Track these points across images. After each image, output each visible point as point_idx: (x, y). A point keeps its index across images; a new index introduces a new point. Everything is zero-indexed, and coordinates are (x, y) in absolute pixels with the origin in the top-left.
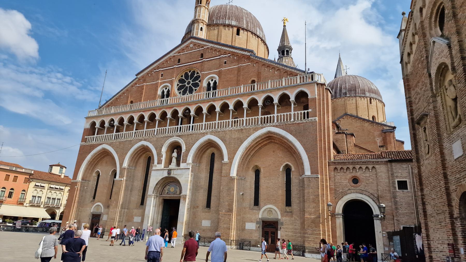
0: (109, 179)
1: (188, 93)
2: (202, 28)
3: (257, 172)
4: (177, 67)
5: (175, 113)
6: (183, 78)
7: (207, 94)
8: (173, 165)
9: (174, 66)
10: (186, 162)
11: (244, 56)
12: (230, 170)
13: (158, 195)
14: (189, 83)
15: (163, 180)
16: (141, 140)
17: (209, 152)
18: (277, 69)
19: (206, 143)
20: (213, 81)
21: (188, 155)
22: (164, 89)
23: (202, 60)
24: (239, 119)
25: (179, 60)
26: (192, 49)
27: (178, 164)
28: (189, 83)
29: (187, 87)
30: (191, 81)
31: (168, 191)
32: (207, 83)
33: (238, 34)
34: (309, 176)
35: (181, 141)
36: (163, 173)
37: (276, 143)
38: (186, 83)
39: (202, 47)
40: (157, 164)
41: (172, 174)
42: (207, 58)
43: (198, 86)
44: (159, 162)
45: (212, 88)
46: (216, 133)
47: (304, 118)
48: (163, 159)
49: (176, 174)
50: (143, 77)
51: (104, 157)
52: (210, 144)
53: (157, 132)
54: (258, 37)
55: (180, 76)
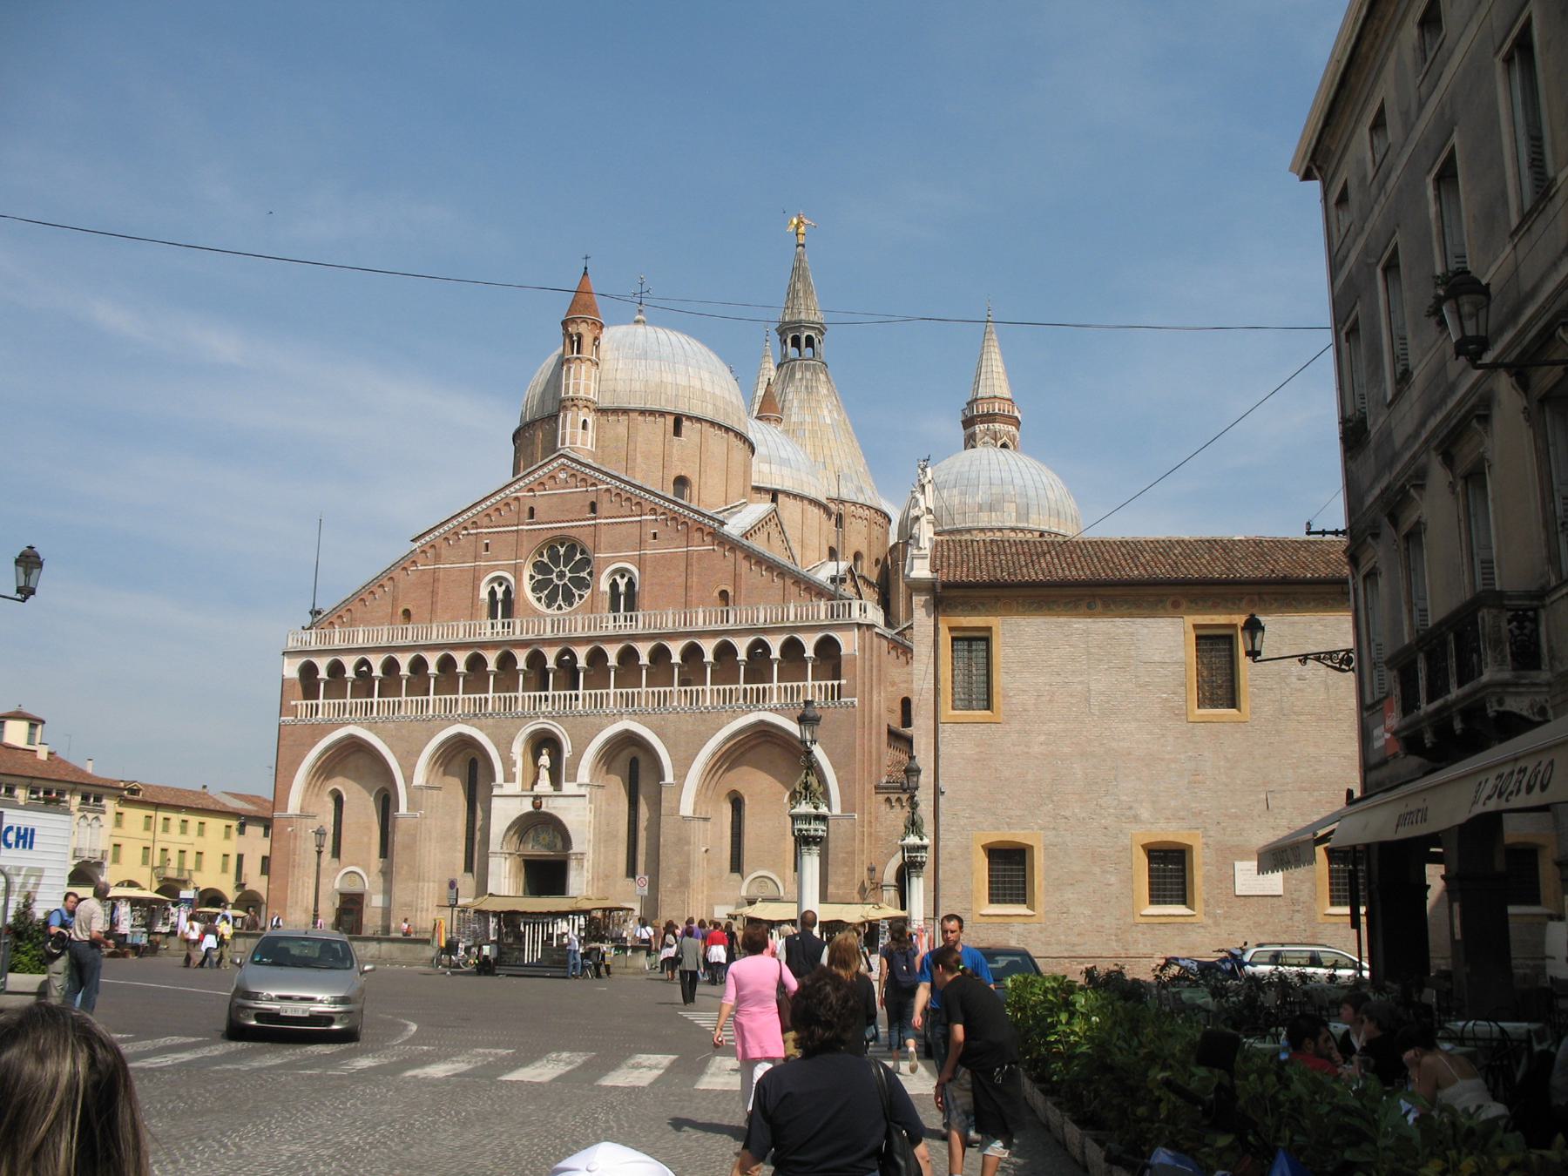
2: (585, 421)
3: (737, 803)
4: (527, 531)
5: (536, 660)
6: (545, 559)
9: (520, 527)
14: (561, 575)
16: (456, 721)
22: (496, 587)
23: (595, 519)
24: (694, 688)
25: (532, 510)
28: (562, 575)
29: (558, 586)
33: (677, 431)
37: (775, 743)
39: (594, 485)
44: (510, 777)
45: (622, 597)
47: (833, 698)
48: (518, 770)
51: (347, 756)
52: (628, 740)
53: (494, 702)
54: (727, 429)
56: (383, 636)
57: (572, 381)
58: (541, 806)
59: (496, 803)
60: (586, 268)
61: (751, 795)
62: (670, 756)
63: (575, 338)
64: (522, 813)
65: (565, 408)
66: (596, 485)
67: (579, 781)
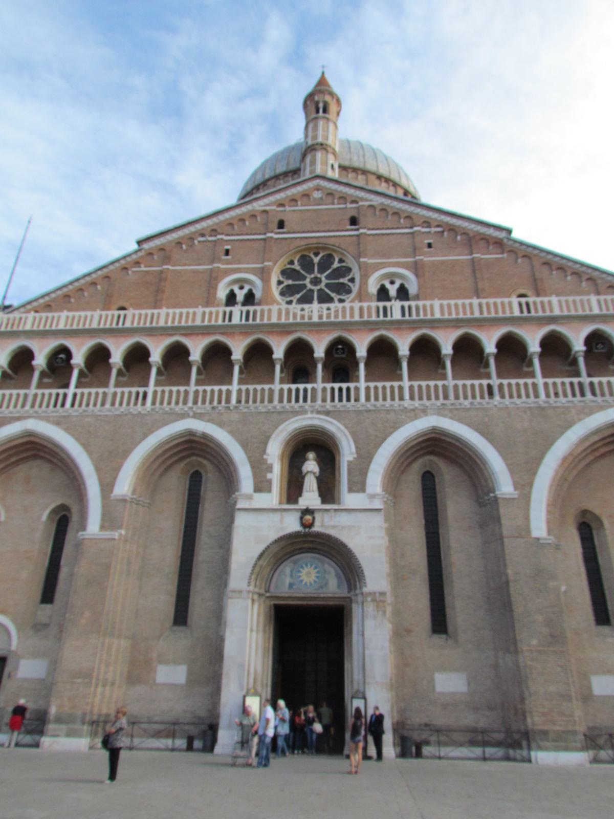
0: (38, 535)
2: (332, 166)
4: (277, 239)
6: (297, 266)
7: (403, 308)
8: (310, 497)
9: (269, 235)
10: (362, 489)
11: (486, 239)
12: (527, 518)
13: (262, 591)
14: (316, 281)
15: (282, 544)
16: (184, 416)
17: (417, 468)
18: (588, 277)
19: (421, 439)
23: (358, 230)
26: (320, 201)
27: (328, 492)
29: (312, 291)
31: (292, 581)
32: (378, 287)
35: (333, 426)
36: (282, 521)
38: (308, 280)
42: (371, 227)
43: (349, 291)
46: (455, 412)
49: (334, 527)
50: (162, 249)
51: (16, 463)
55: (286, 263)
56: (95, 318)
57: (320, 133)
58: (311, 525)
59: (242, 521)
60: (323, 73)
61: (610, 516)
62: (505, 459)
64: (281, 534)
65: (315, 150)
66: (357, 202)
67: (370, 489)
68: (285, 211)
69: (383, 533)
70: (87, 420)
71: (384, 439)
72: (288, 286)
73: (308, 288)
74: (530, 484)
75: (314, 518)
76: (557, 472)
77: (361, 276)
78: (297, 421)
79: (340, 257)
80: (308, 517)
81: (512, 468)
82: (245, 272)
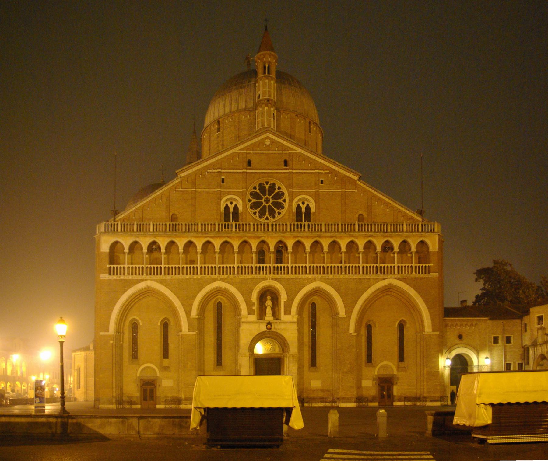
1: (268, 216)
8: (269, 317)
10: (289, 313)
12: (349, 326)
14: (267, 201)
15: (260, 335)
16: (215, 280)
20: (305, 205)
21: (292, 305)
28: (267, 201)
29: (265, 206)
30: (271, 199)
32: (297, 206)
34: (430, 332)
35: (278, 286)
36: (259, 327)
38: (263, 199)
40: (248, 314)
41: (273, 328)
43: (283, 208)
48: (255, 308)
49: (279, 329)
55: (252, 188)
58: (270, 329)
59: (244, 327)
62: (343, 301)
63: (267, 65)
67: (292, 313)
68: (251, 153)
69: (296, 332)
70: (174, 281)
71: (299, 292)
72: (254, 203)
73: (264, 204)
74: (352, 312)
75: (271, 326)
76: (362, 306)
77: (289, 200)
78: (264, 283)
79: (279, 185)
80: (269, 326)
81: (346, 305)
82: (233, 195)
